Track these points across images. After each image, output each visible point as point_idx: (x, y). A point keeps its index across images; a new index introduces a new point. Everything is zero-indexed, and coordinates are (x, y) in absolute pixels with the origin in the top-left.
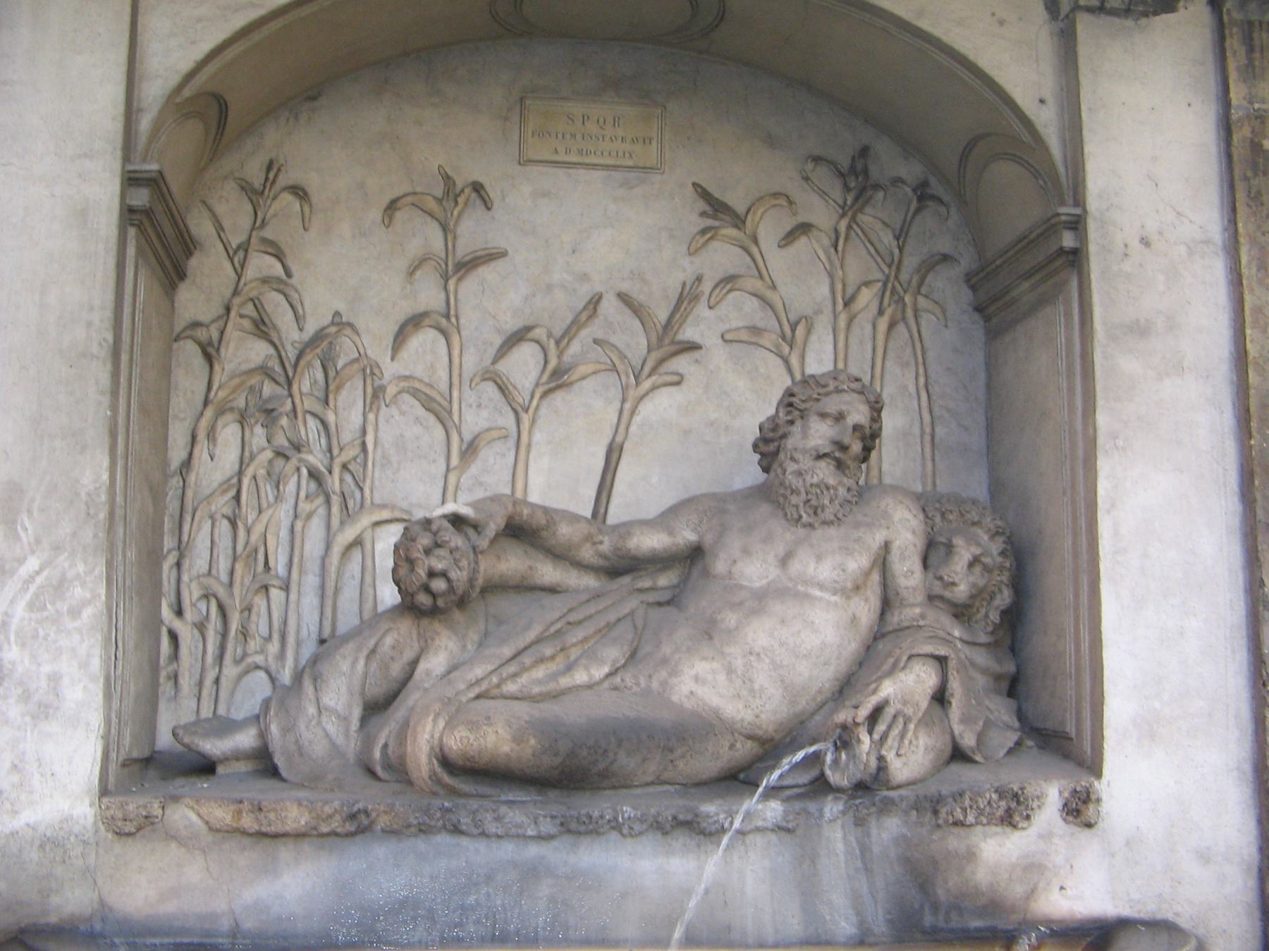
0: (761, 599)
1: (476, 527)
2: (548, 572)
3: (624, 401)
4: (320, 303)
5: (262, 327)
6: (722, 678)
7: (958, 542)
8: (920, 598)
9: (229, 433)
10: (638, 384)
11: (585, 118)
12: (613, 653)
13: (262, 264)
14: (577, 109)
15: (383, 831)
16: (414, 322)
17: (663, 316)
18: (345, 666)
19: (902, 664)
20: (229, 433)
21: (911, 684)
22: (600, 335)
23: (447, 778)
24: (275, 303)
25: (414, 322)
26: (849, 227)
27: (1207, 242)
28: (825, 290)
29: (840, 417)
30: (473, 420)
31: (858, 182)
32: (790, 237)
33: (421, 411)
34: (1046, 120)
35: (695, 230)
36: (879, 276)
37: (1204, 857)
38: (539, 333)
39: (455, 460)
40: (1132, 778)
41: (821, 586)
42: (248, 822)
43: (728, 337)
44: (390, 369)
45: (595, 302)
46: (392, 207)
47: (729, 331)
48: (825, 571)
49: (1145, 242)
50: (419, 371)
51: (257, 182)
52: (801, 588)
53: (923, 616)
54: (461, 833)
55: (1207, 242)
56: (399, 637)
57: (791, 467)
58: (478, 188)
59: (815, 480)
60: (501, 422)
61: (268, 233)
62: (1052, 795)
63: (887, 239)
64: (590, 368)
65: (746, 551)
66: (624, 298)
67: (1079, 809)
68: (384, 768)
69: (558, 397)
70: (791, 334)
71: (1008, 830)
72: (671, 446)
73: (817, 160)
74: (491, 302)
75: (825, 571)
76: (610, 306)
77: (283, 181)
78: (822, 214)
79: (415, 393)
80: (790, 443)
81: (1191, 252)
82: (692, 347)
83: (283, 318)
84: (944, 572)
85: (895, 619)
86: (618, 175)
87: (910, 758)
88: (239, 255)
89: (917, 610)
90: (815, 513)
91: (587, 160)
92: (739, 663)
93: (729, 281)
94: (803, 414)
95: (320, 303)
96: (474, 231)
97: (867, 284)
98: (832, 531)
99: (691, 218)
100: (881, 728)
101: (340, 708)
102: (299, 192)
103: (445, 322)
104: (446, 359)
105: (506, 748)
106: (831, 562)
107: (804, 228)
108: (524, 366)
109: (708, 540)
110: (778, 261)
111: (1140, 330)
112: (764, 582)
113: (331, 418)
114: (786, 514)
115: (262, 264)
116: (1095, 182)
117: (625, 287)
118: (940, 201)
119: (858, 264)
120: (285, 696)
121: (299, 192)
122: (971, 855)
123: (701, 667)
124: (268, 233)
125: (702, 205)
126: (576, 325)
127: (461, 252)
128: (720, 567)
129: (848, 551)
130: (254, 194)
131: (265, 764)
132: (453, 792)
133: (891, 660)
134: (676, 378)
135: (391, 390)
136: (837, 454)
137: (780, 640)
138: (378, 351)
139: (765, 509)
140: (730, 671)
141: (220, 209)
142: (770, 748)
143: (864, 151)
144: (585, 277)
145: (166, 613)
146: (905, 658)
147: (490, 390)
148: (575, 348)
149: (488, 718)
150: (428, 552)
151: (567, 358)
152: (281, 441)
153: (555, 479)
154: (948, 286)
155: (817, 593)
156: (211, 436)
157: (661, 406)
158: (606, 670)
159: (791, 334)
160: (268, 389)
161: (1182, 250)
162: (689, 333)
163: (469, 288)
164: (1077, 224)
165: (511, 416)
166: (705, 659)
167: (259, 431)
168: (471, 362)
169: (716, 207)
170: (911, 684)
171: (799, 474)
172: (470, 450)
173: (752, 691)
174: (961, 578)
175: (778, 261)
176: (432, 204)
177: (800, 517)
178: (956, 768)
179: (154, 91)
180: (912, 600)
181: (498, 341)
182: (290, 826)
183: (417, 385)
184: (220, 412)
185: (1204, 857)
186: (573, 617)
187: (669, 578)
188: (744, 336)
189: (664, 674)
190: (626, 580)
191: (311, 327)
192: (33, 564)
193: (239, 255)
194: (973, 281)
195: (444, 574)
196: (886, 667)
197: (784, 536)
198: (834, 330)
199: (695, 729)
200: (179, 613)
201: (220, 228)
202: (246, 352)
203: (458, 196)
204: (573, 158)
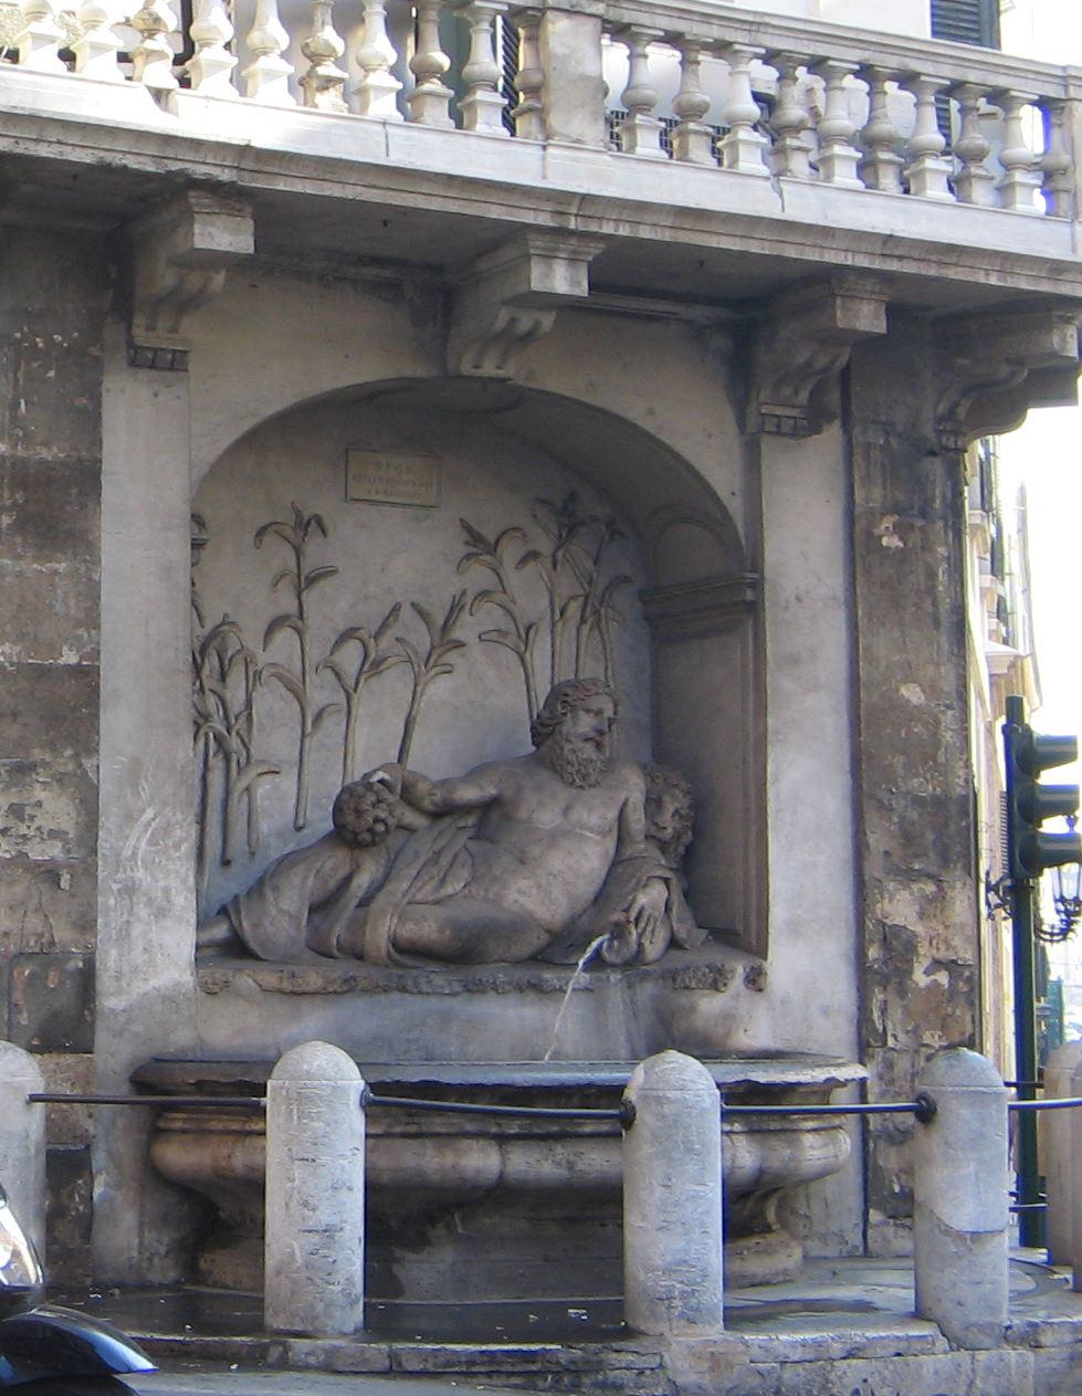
0: (554, 838)
3: (415, 686)
6: (534, 891)
7: (666, 799)
8: (642, 837)
10: (428, 672)
12: (465, 874)
15: (362, 990)
17: (440, 621)
18: (297, 881)
19: (643, 882)
22: (399, 635)
23: (397, 957)
27: (835, 598)
28: (545, 602)
29: (599, 713)
31: (569, 523)
32: (523, 561)
33: (283, 690)
35: (462, 555)
36: (582, 592)
37: (825, 1012)
38: (363, 634)
39: (309, 729)
40: (786, 960)
41: (592, 831)
42: (286, 985)
43: (483, 637)
44: (262, 658)
45: (396, 609)
46: (261, 532)
47: (484, 633)
48: (594, 819)
49: (798, 599)
50: (280, 659)
52: (578, 830)
53: (646, 850)
54: (407, 991)
56: (335, 862)
57: (568, 747)
58: (319, 520)
59: (585, 756)
62: (740, 970)
63: (589, 564)
64: (395, 659)
65: (540, 804)
67: (755, 980)
68: (339, 950)
71: (713, 992)
74: (329, 608)
75: (594, 819)
76: (407, 613)
78: (544, 545)
79: (280, 677)
80: (565, 729)
82: (459, 645)
84: (659, 820)
85: (628, 852)
89: (642, 846)
90: (584, 779)
91: (390, 499)
93: (484, 594)
94: (574, 709)
97: (572, 598)
98: (594, 791)
100: (642, 925)
101: (292, 909)
103: (295, 621)
104: (299, 651)
105: (434, 936)
106: (596, 814)
107: (532, 555)
109: (508, 793)
110: (516, 580)
111: (793, 660)
112: (552, 826)
113: (228, 695)
114: (563, 778)
116: (770, 557)
117: (416, 598)
118: (621, 533)
119: (567, 584)
122: (693, 1008)
123: (523, 883)
125: (465, 536)
126: (384, 626)
127: (305, 571)
128: (523, 814)
132: (397, 964)
133: (634, 880)
134: (449, 668)
136: (598, 738)
137: (560, 869)
138: (253, 641)
139: (544, 775)
140: (539, 887)
143: (573, 496)
146: (645, 878)
147: (329, 675)
149: (424, 917)
150: (374, 806)
154: (625, 600)
155: (589, 834)
157: (439, 689)
158: (463, 884)
162: (457, 634)
163: (310, 598)
164: (758, 585)
165: (343, 694)
166: (525, 878)
168: (315, 653)
169: (474, 537)
170: (651, 897)
171: (574, 751)
173: (551, 901)
174: (669, 824)
175: (516, 580)
176: (289, 532)
177: (574, 781)
178: (676, 954)
180: (638, 839)
181: (333, 638)
183: (281, 671)
185: (825, 1012)
186: (437, 847)
188: (494, 636)
189: (496, 888)
190: (448, 820)
191: (210, 625)
192: (149, 813)
194: (645, 596)
195: (383, 821)
196: (631, 885)
197: (564, 794)
198: (552, 632)
199: (518, 925)
203: (309, 525)
204: (381, 497)
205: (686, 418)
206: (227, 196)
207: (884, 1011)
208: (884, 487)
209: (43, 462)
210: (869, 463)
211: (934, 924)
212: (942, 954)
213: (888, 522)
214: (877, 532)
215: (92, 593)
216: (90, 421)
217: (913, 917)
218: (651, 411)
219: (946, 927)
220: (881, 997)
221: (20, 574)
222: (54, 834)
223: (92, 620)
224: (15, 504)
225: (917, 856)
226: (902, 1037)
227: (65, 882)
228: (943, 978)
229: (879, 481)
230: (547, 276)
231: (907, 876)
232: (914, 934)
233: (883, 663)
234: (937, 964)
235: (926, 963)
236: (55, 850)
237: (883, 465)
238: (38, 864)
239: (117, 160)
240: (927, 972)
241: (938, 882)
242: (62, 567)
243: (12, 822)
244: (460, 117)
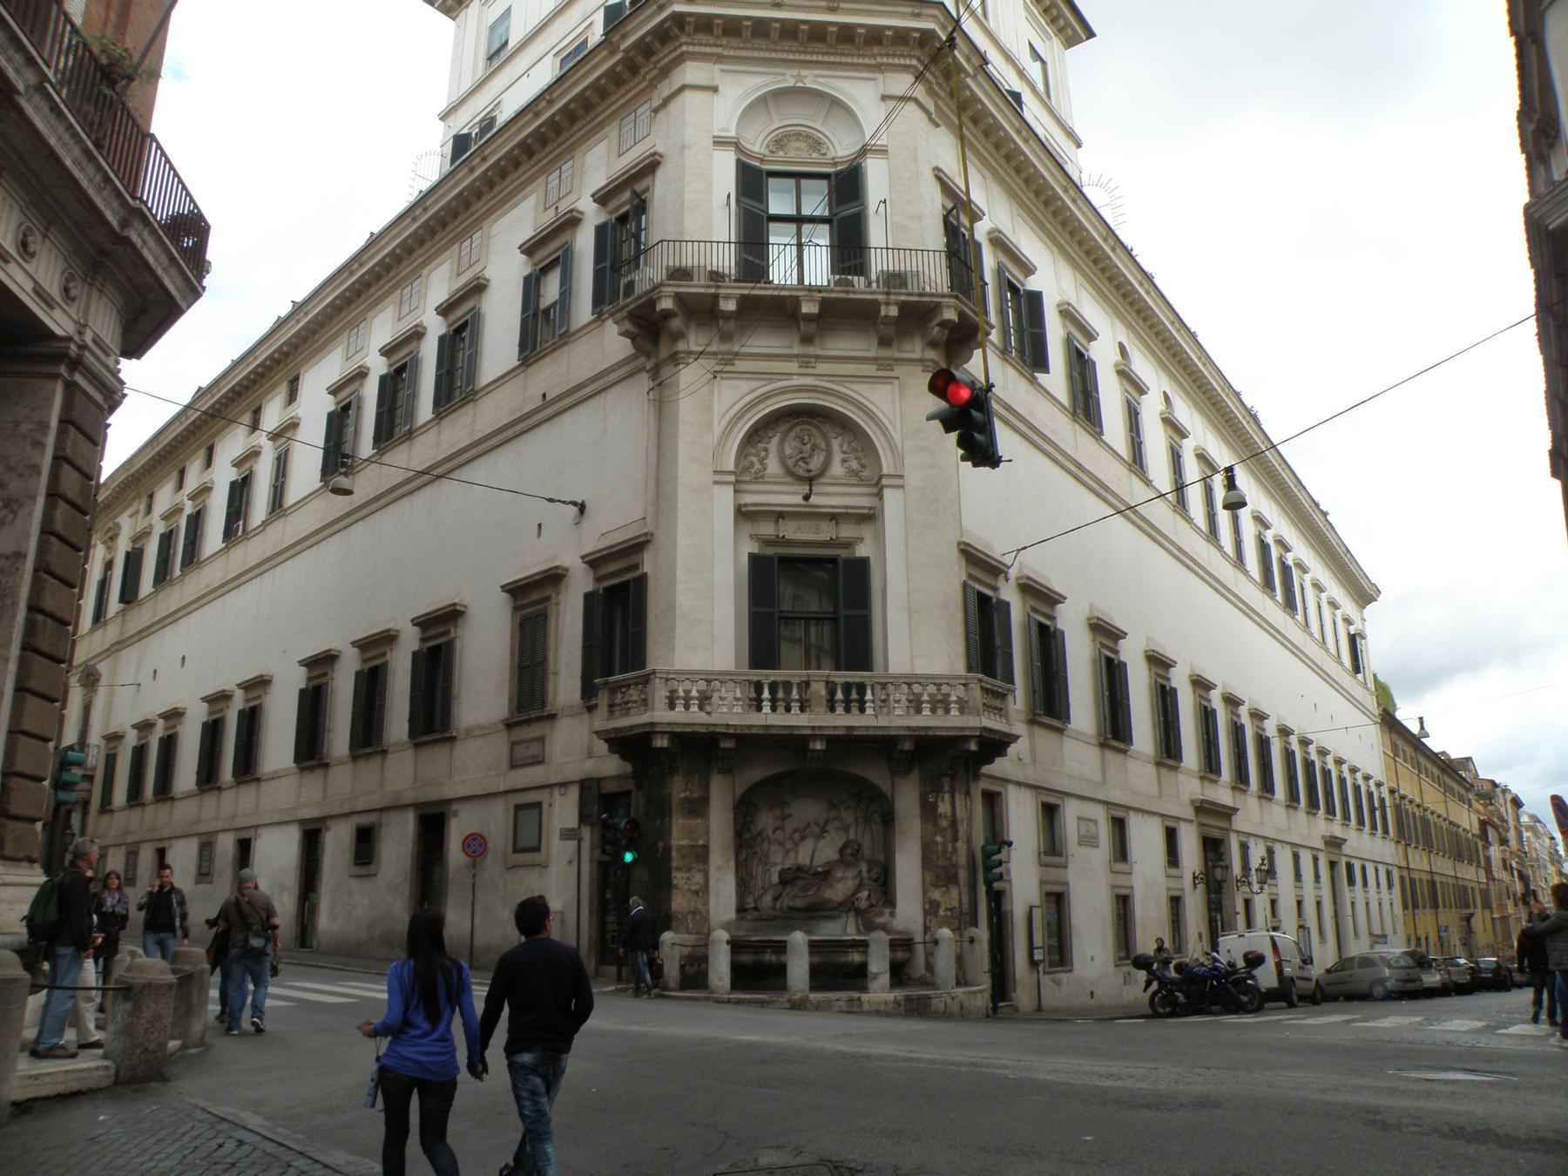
0: (839, 881)
5: (749, 830)
21: (865, 894)
34: (889, 794)
70: (846, 828)
72: (826, 851)
74: (790, 825)
87: (863, 905)
96: (787, 811)
106: (851, 873)
108: (797, 836)
110: (844, 814)
116: (897, 806)
120: (760, 898)
131: (756, 909)
142: (841, 904)
153: (803, 856)
154: (877, 818)
157: (822, 843)
159: (846, 828)
170: (865, 894)
174: (874, 875)
187: (824, 876)
203: (784, 804)
206: (727, 736)
215: (708, 827)
216: (707, 788)
223: (707, 833)
231: (937, 886)
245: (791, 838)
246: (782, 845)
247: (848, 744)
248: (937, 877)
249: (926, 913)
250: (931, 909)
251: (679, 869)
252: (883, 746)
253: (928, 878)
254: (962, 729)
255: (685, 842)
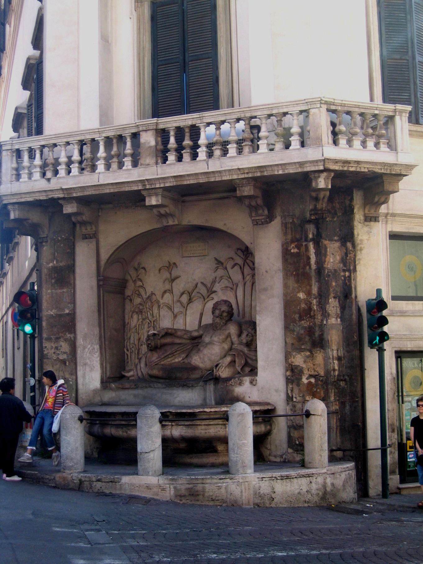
1: (159, 335)
2: (178, 341)
4: (149, 290)
5: (139, 295)
6: (199, 360)
9: (135, 316)
11: (193, 247)
12: (184, 356)
13: (139, 283)
14: (192, 245)
16: (165, 292)
17: (209, 286)
20: (135, 316)
24: (141, 290)
25: (165, 292)
26: (244, 264)
27: (279, 270)
29: (220, 309)
30: (176, 310)
37: (277, 391)
44: (161, 302)
46: (160, 270)
49: (267, 272)
51: (136, 267)
55: (279, 270)
58: (175, 264)
60: (181, 310)
61: (139, 277)
66: (202, 283)
69: (191, 304)
73: (238, 249)
74: (179, 286)
75: (215, 339)
77: (141, 266)
78: (240, 261)
81: (276, 272)
82: (215, 292)
83: (143, 293)
85: (233, 347)
86: (200, 258)
88: (135, 282)
92: (202, 357)
93: (221, 277)
95: (149, 290)
96: (175, 273)
98: (219, 331)
99: (214, 265)
100: (218, 368)
102: (144, 268)
103: (171, 291)
107: (235, 264)
108: (185, 299)
111: (265, 290)
115: (139, 283)
117: (202, 281)
121: (144, 268)
122: (233, 391)
124: (139, 277)
125: (216, 262)
127: (172, 278)
129: (220, 335)
130: (136, 270)
135: (162, 306)
138: (159, 298)
140: (200, 358)
141: (131, 273)
144: (194, 280)
145: (125, 351)
147: (179, 304)
148: (193, 294)
151: (192, 296)
152: (144, 317)
156: (132, 317)
160: (141, 307)
161: (274, 272)
162: (214, 289)
163: (174, 284)
167: (140, 315)
169: (219, 262)
172: (175, 316)
175: (231, 271)
179: (103, 263)
181: (180, 294)
182: (127, 387)
184: (133, 313)
185: (277, 391)
191: (148, 295)
193: (135, 282)
199: (195, 368)
200: (128, 351)
201: (131, 277)
202: (137, 301)
203: (171, 266)
205: (236, 222)
206: (69, 200)
207: (292, 391)
208: (292, 234)
209: (60, 266)
210: (286, 228)
211: (309, 364)
212: (313, 373)
213: (293, 245)
214: (289, 248)
216: (72, 255)
217: (302, 362)
218: (225, 224)
219: (314, 365)
220: (291, 386)
221: (56, 293)
222: (65, 353)
223: (73, 301)
224: (55, 277)
225: (303, 344)
226: (298, 398)
227: (67, 364)
228: (313, 380)
229: (290, 233)
230: (150, 201)
231: (300, 350)
232: (302, 368)
233: (291, 288)
234: (311, 376)
235: (307, 376)
236: (65, 356)
237: (291, 228)
238: (61, 360)
239: (38, 198)
240: (307, 379)
241: (311, 352)
242: (65, 290)
243: (56, 351)
244: (121, 165)
245: (179, 301)
246: (170, 308)
247: (185, 193)
248: (300, 339)
249: (288, 381)
250: (293, 375)
251: (49, 339)
252: (221, 191)
253: (289, 341)
254: (301, 164)
255: (52, 312)
